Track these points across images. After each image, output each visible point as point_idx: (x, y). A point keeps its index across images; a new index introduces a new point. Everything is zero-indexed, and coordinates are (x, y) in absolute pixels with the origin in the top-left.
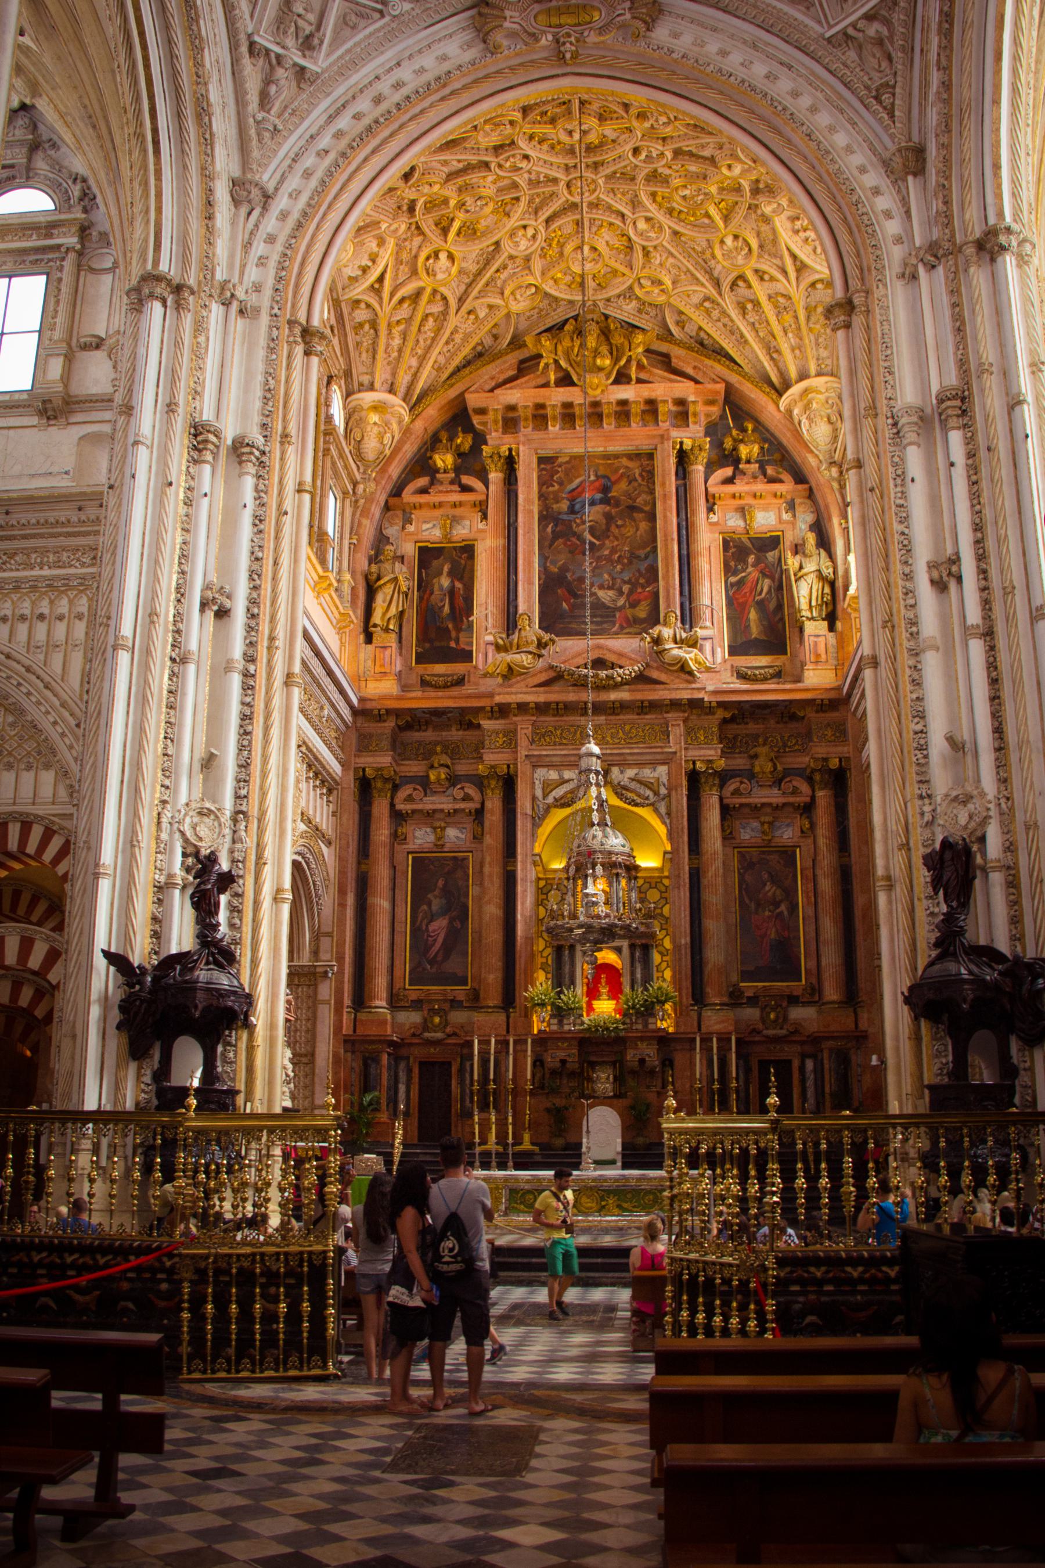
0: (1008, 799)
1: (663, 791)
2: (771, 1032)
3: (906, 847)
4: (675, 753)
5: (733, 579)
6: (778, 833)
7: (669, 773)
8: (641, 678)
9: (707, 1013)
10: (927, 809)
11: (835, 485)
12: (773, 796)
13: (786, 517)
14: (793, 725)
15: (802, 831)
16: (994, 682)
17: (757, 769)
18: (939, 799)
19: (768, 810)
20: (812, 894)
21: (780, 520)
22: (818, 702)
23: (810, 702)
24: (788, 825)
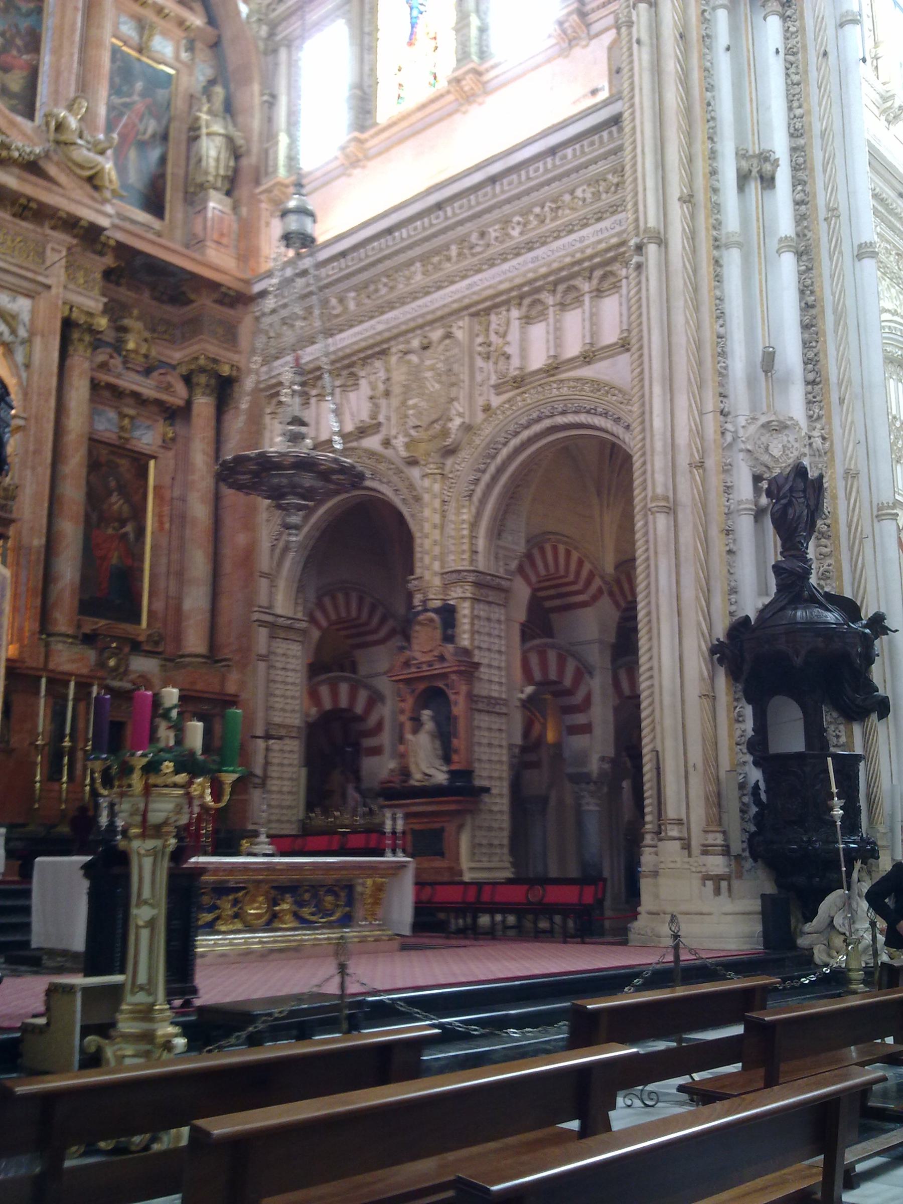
0: (824, 439)
1: (22, 333)
2: (116, 684)
3: (701, 465)
4: (48, 287)
5: (117, 100)
6: (137, 434)
7: (33, 312)
8: (32, 167)
9: (58, 646)
10: (729, 426)
11: (261, 45)
12: (147, 388)
13: (184, 56)
14: (169, 308)
15: (164, 441)
16: (807, 307)
17: (131, 345)
18: (742, 421)
19: (130, 401)
20: (166, 519)
21: (177, 57)
22: (223, 289)
23: (214, 286)
24: (148, 427)
